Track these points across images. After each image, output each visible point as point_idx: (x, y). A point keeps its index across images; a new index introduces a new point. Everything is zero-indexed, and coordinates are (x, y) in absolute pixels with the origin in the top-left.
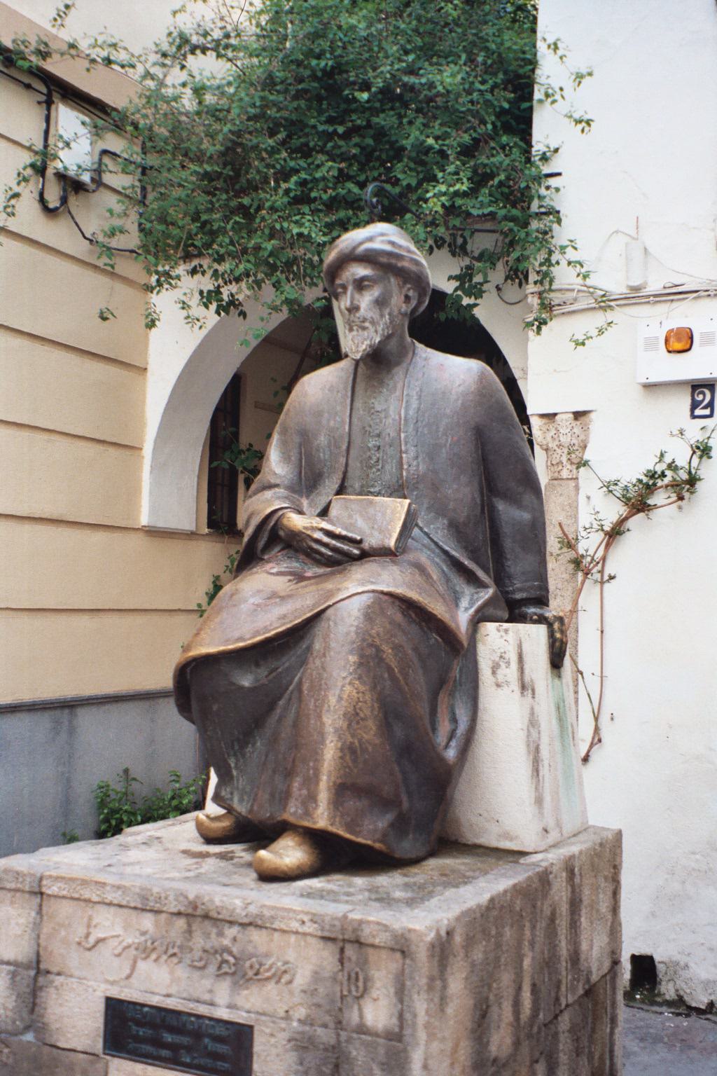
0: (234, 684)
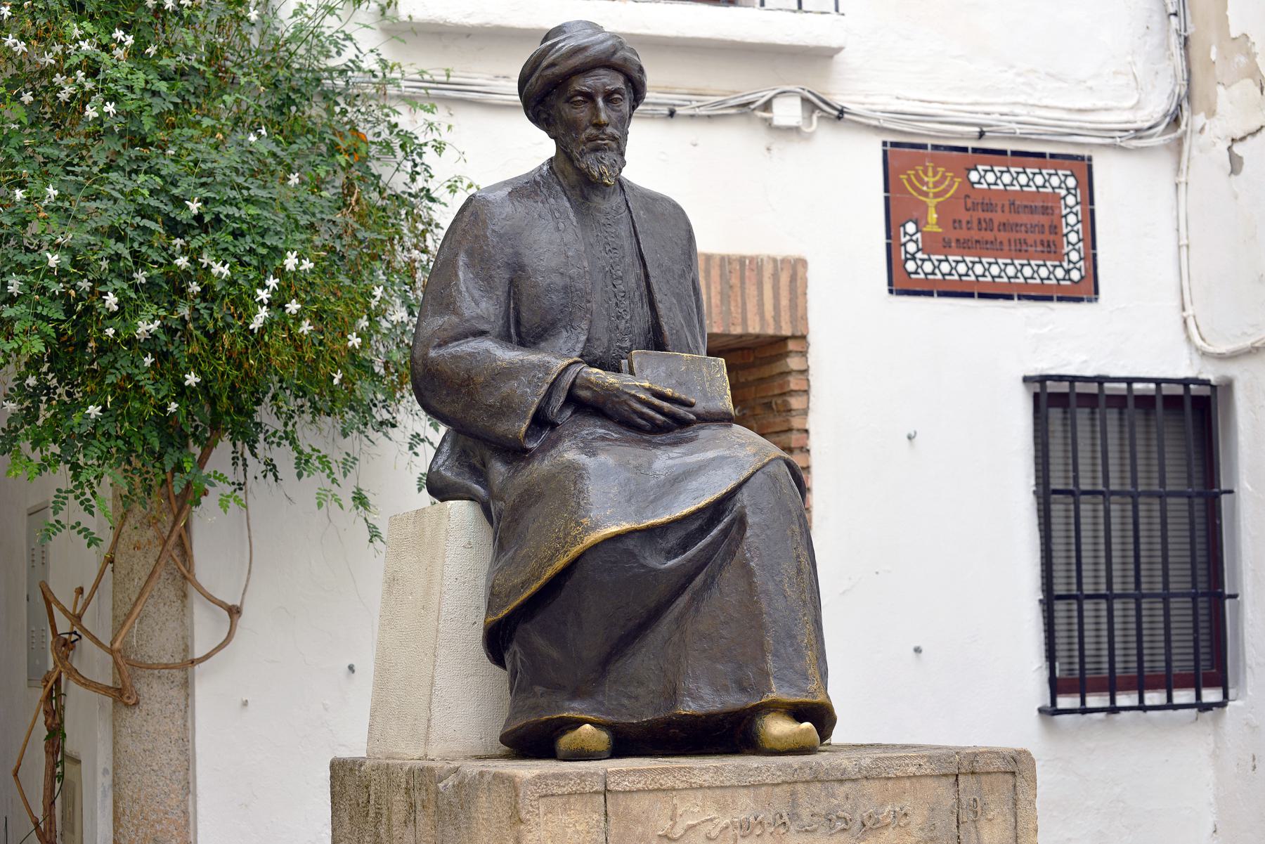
0: (644, 566)
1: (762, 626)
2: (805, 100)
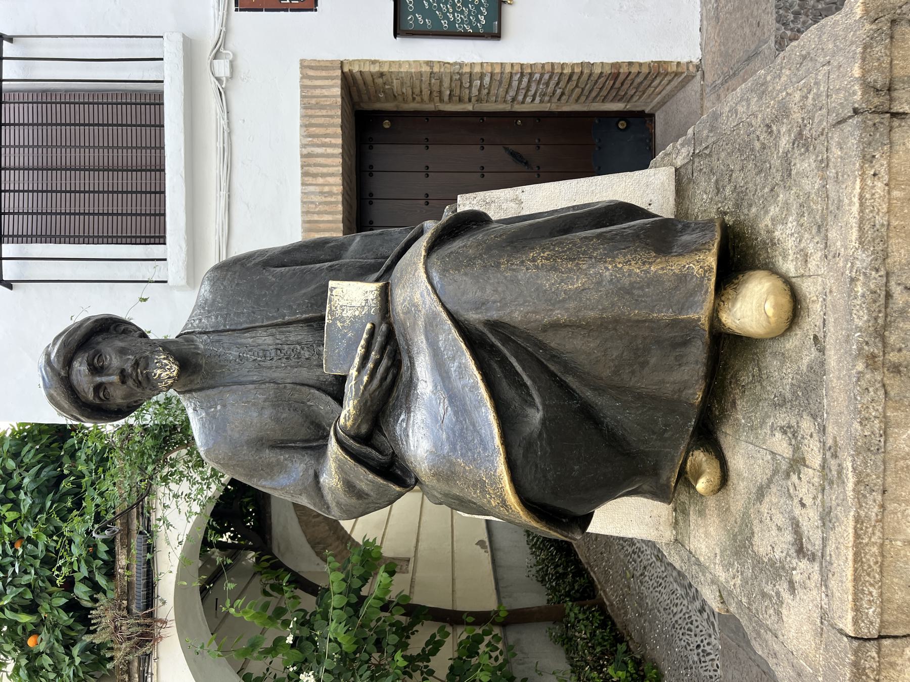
0: (540, 434)
1: (616, 321)
2: (215, 58)
